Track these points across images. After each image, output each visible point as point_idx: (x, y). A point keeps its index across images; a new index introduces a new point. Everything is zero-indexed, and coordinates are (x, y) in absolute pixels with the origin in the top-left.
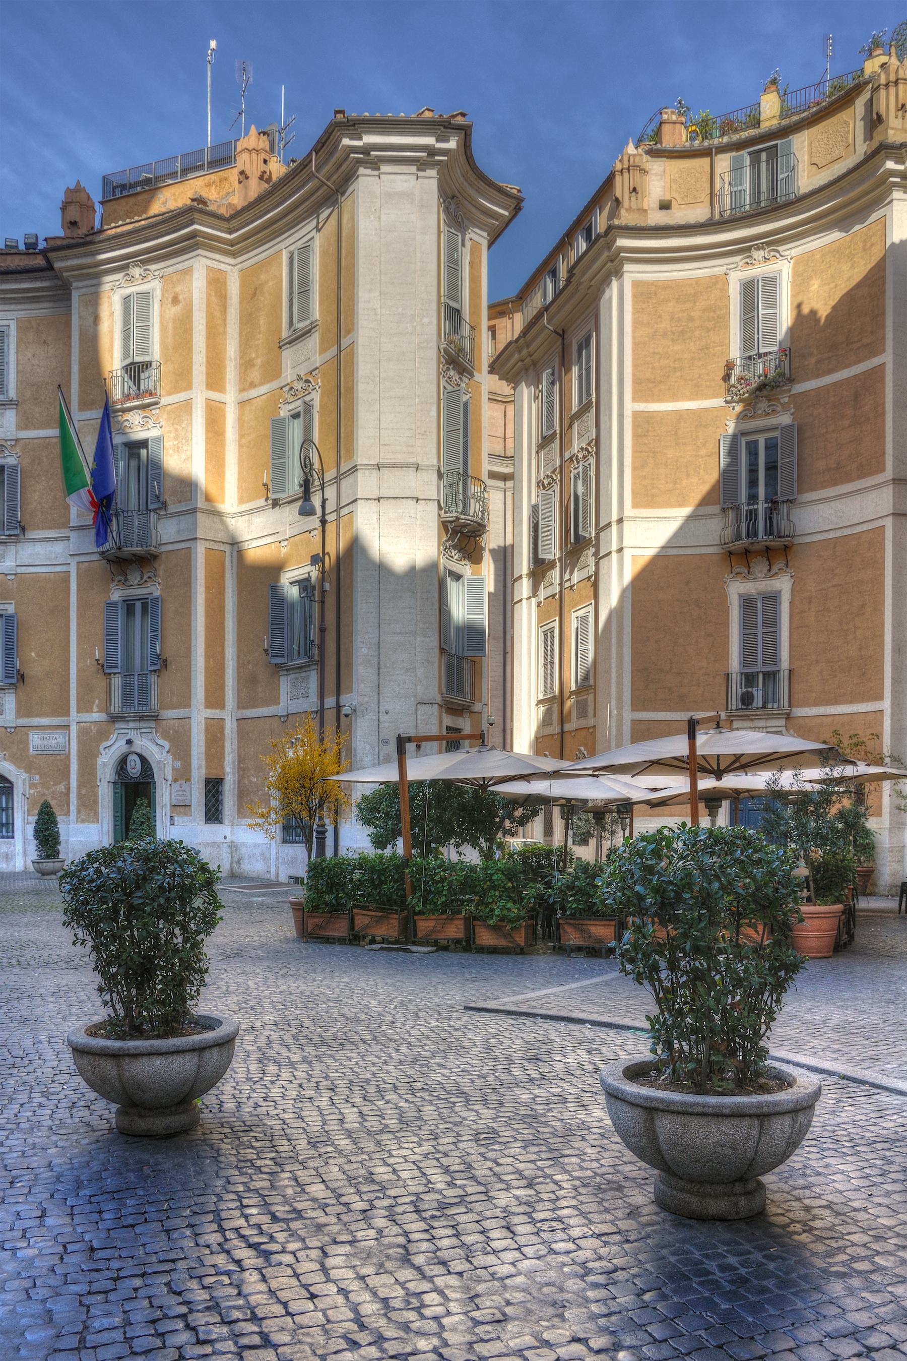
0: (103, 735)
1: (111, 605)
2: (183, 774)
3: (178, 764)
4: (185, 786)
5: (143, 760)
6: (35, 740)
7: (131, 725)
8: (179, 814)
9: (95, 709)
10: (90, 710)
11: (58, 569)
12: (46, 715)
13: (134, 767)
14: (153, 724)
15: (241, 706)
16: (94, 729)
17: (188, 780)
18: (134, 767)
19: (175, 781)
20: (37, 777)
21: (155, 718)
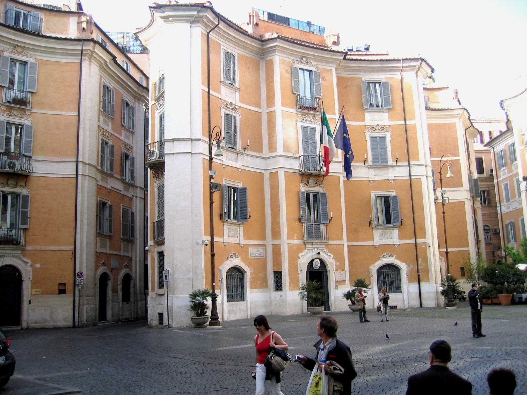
0: (299, 249)
1: (299, 193)
2: (340, 268)
3: (338, 263)
4: (343, 272)
5: (322, 262)
6: (251, 250)
7: (315, 246)
8: (339, 284)
9: (295, 238)
10: (293, 238)
11: (258, 171)
12: (256, 239)
13: (317, 265)
14: (323, 246)
15: (349, 240)
16: (295, 248)
17: (344, 270)
18: (317, 265)
19: (337, 270)
20: (252, 269)
21: (325, 243)
